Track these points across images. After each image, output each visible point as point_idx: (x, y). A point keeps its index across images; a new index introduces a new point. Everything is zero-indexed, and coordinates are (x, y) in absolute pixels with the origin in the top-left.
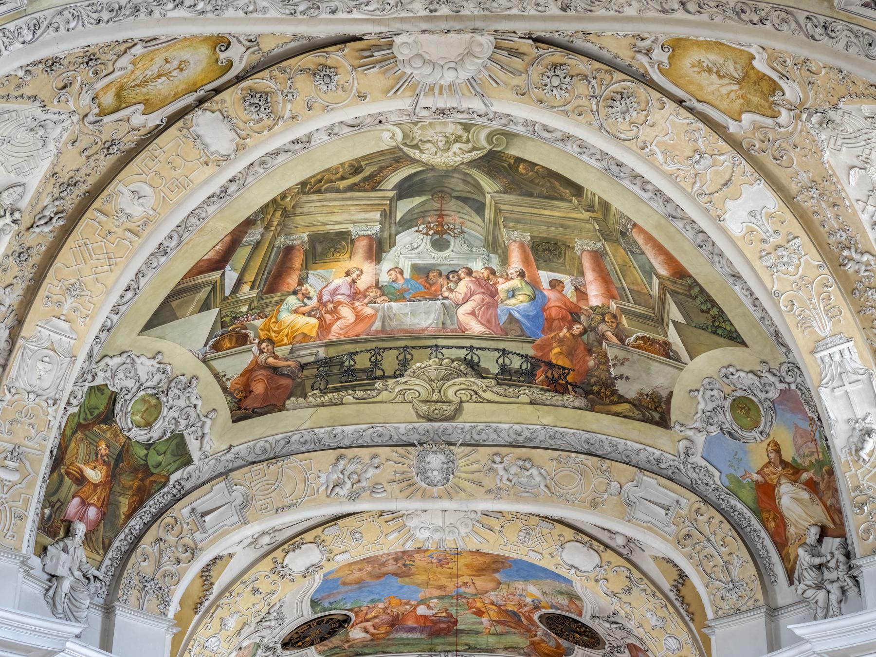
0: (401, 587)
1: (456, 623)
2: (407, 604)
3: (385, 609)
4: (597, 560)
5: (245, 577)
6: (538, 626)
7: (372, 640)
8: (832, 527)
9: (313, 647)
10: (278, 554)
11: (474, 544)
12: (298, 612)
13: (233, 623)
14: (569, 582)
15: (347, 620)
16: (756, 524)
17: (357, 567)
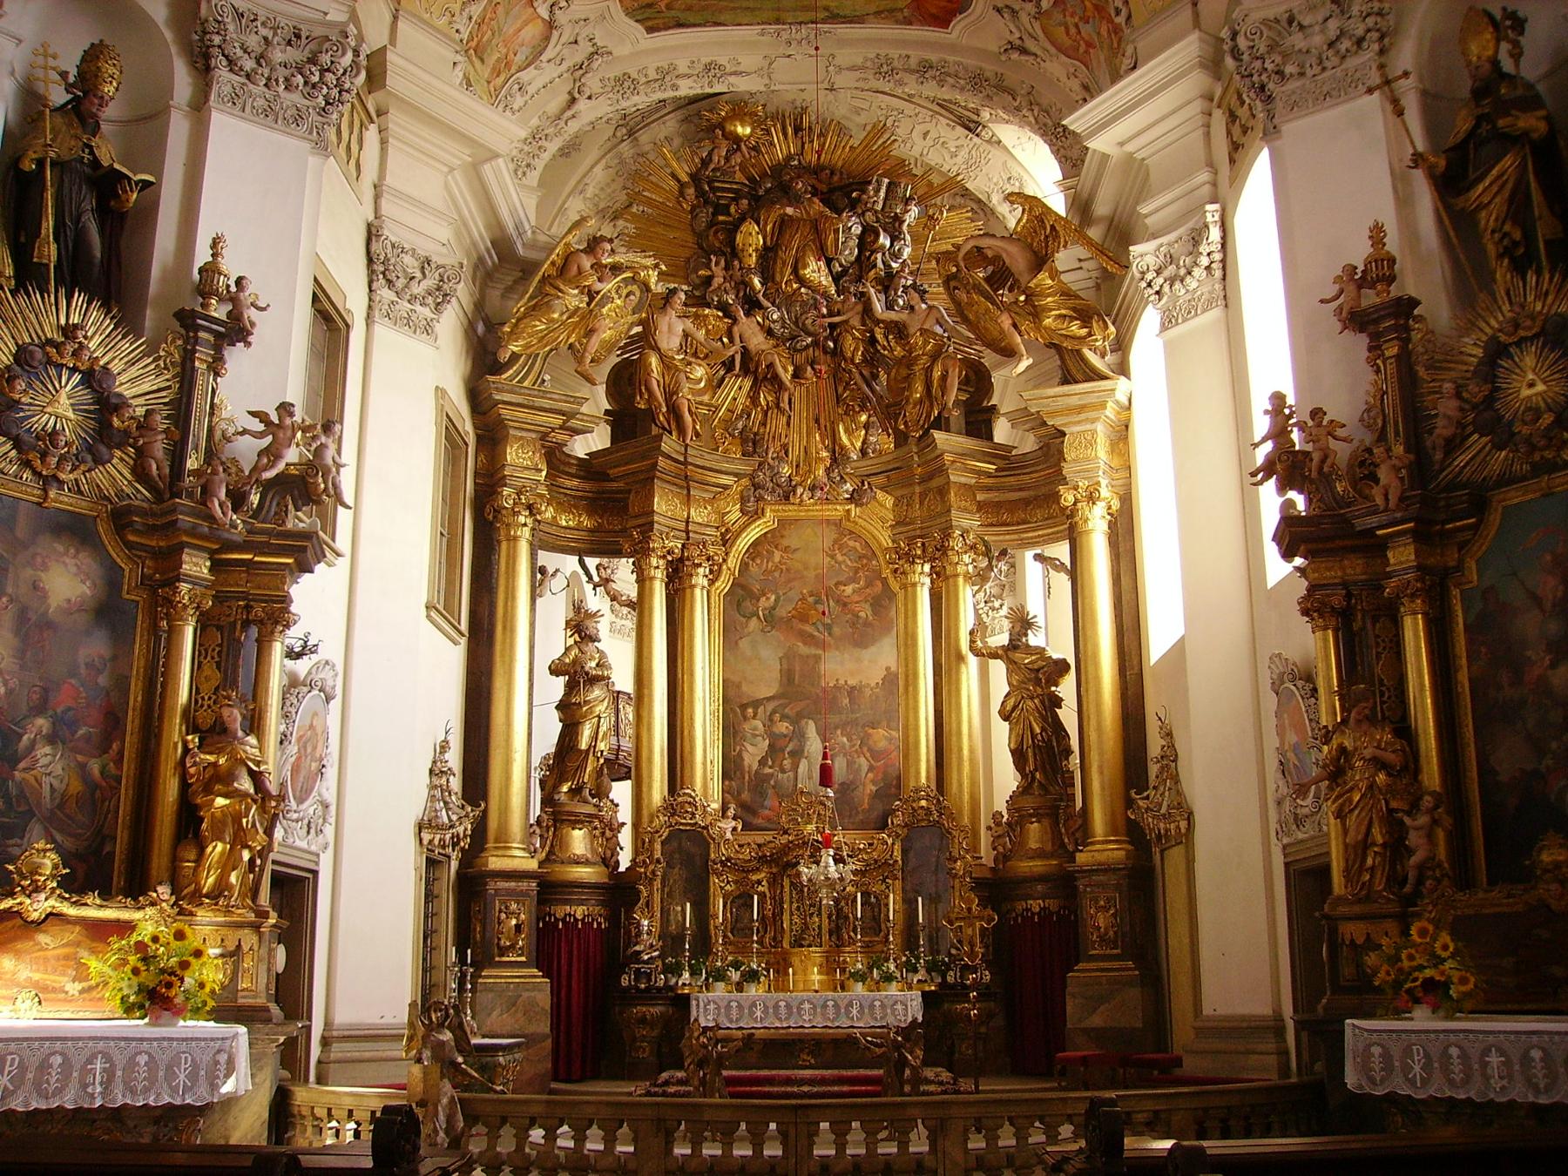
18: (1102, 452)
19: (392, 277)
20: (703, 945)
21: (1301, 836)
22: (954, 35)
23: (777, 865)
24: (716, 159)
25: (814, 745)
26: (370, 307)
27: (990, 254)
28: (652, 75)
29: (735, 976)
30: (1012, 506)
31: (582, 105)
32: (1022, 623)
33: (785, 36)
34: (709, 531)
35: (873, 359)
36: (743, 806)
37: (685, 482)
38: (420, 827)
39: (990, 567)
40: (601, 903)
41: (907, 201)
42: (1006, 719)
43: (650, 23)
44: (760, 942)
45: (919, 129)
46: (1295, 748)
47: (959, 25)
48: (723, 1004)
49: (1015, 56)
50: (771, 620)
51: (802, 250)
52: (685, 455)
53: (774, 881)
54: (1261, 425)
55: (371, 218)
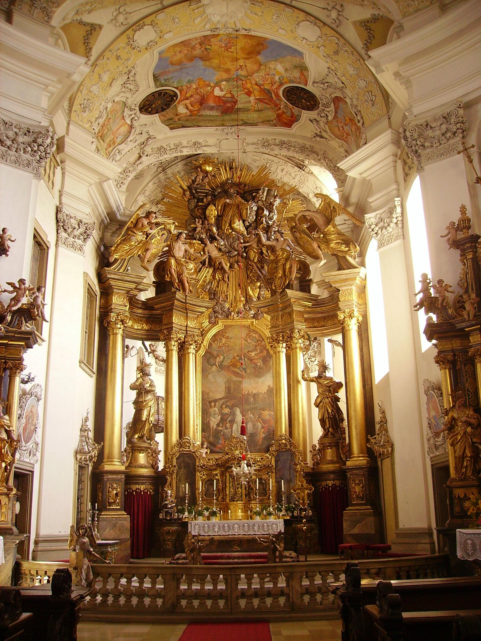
1: (236, 102)
2: (209, 85)
3: (197, 89)
4: (319, 33)
5: (111, 48)
6: (281, 100)
7: (190, 116)
9: (157, 115)
10: (130, 32)
12: (147, 88)
13: (106, 78)
14: (300, 54)
17: (178, 49)
18: (355, 297)
19: (66, 228)
20: (193, 501)
21: (438, 453)
22: (293, 131)
23: (224, 468)
24: (198, 180)
25: (239, 418)
26: (57, 240)
27: (309, 218)
28: (172, 147)
29: (206, 513)
30: (318, 320)
31: (144, 158)
32: (324, 367)
33: (226, 131)
34: (195, 330)
35: (262, 260)
36: (210, 443)
37: (186, 310)
38: (76, 453)
39: (310, 345)
40: (151, 484)
41: (275, 197)
42: (317, 406)
43: (171, 126)
44: (217, 500)
45: (280, 168)
46: (434, 418)
47: (296, 127)
48: (201, 525)
49: (318, 139)
50: (221, 367)
51: (233, 216)
52: (186, 299)
53: (223, 474)
54: (418, 287)
55: (58, 204)
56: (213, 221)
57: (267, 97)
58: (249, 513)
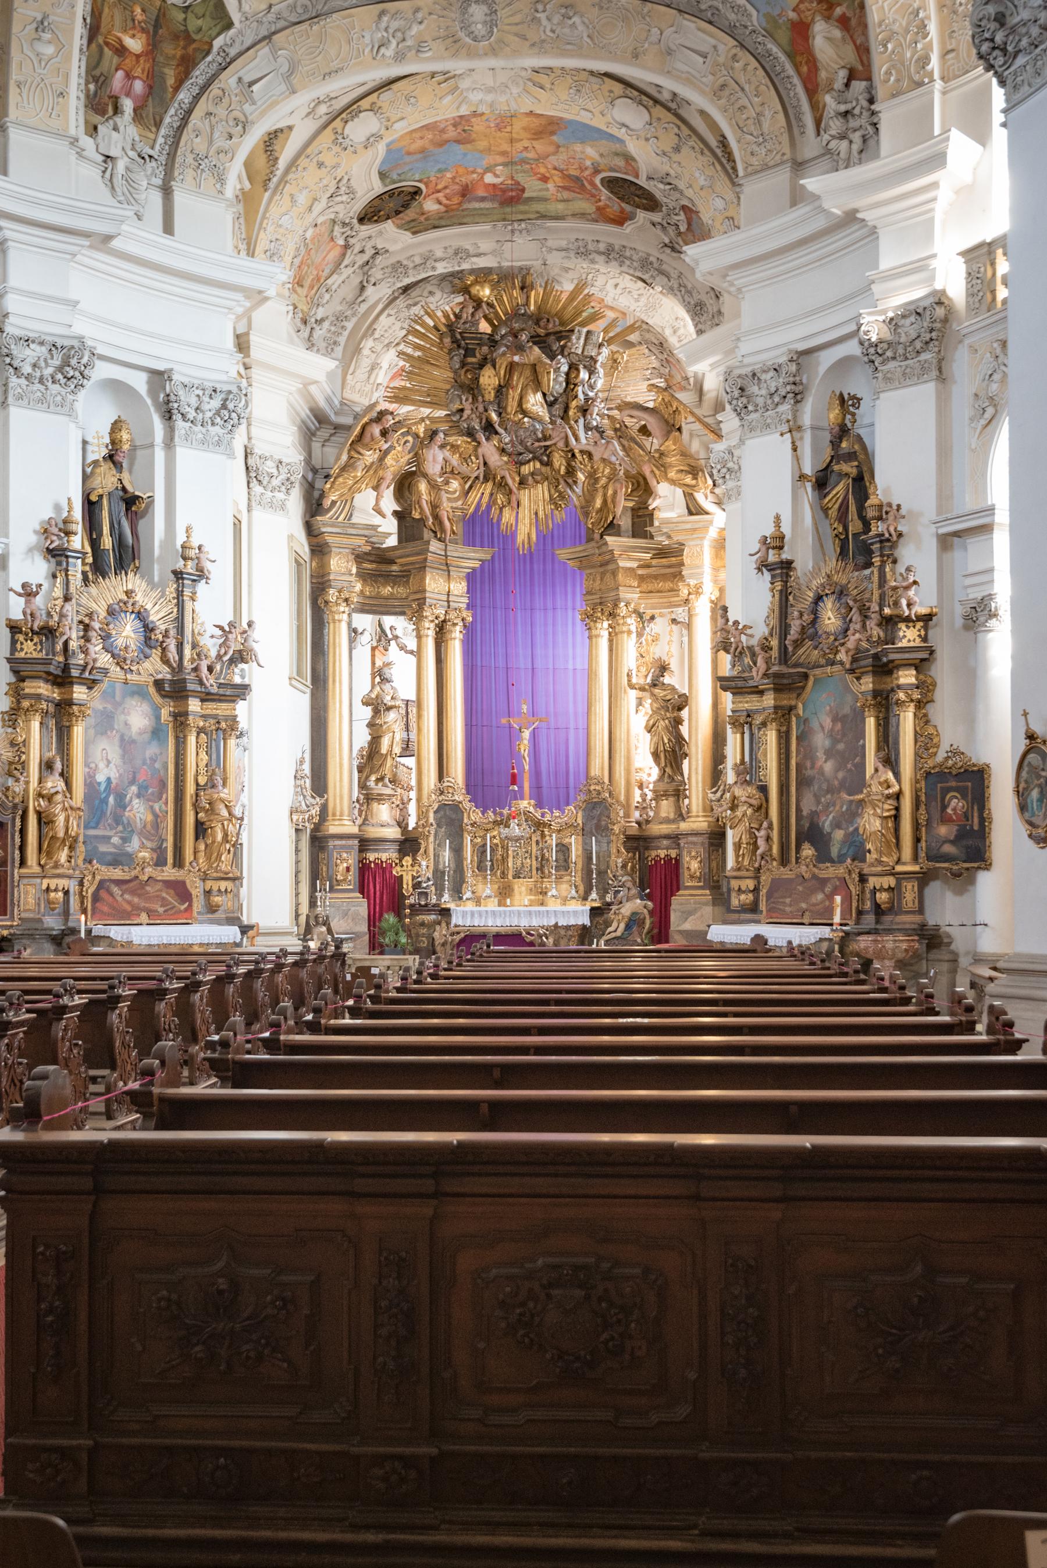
0: (465, 155)
1: (523, 190)
4: (647, 117)
8: (860, 71)
11: (527, 104)
15: (417, 192)
16: (790, 70)
24: (465, 316)
37: (447, 568)
41: (600, 345)
47: (629, 228)
52: (446, 550)
56: (491, 396)
57: (575, 184)
58: (505, 893)
